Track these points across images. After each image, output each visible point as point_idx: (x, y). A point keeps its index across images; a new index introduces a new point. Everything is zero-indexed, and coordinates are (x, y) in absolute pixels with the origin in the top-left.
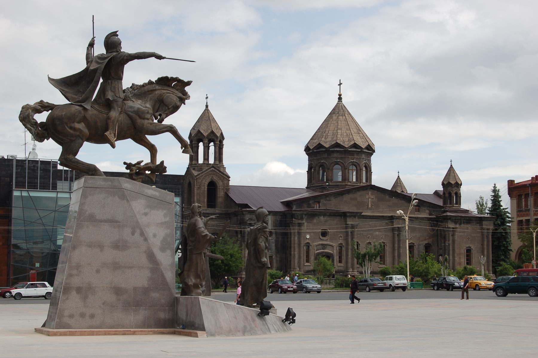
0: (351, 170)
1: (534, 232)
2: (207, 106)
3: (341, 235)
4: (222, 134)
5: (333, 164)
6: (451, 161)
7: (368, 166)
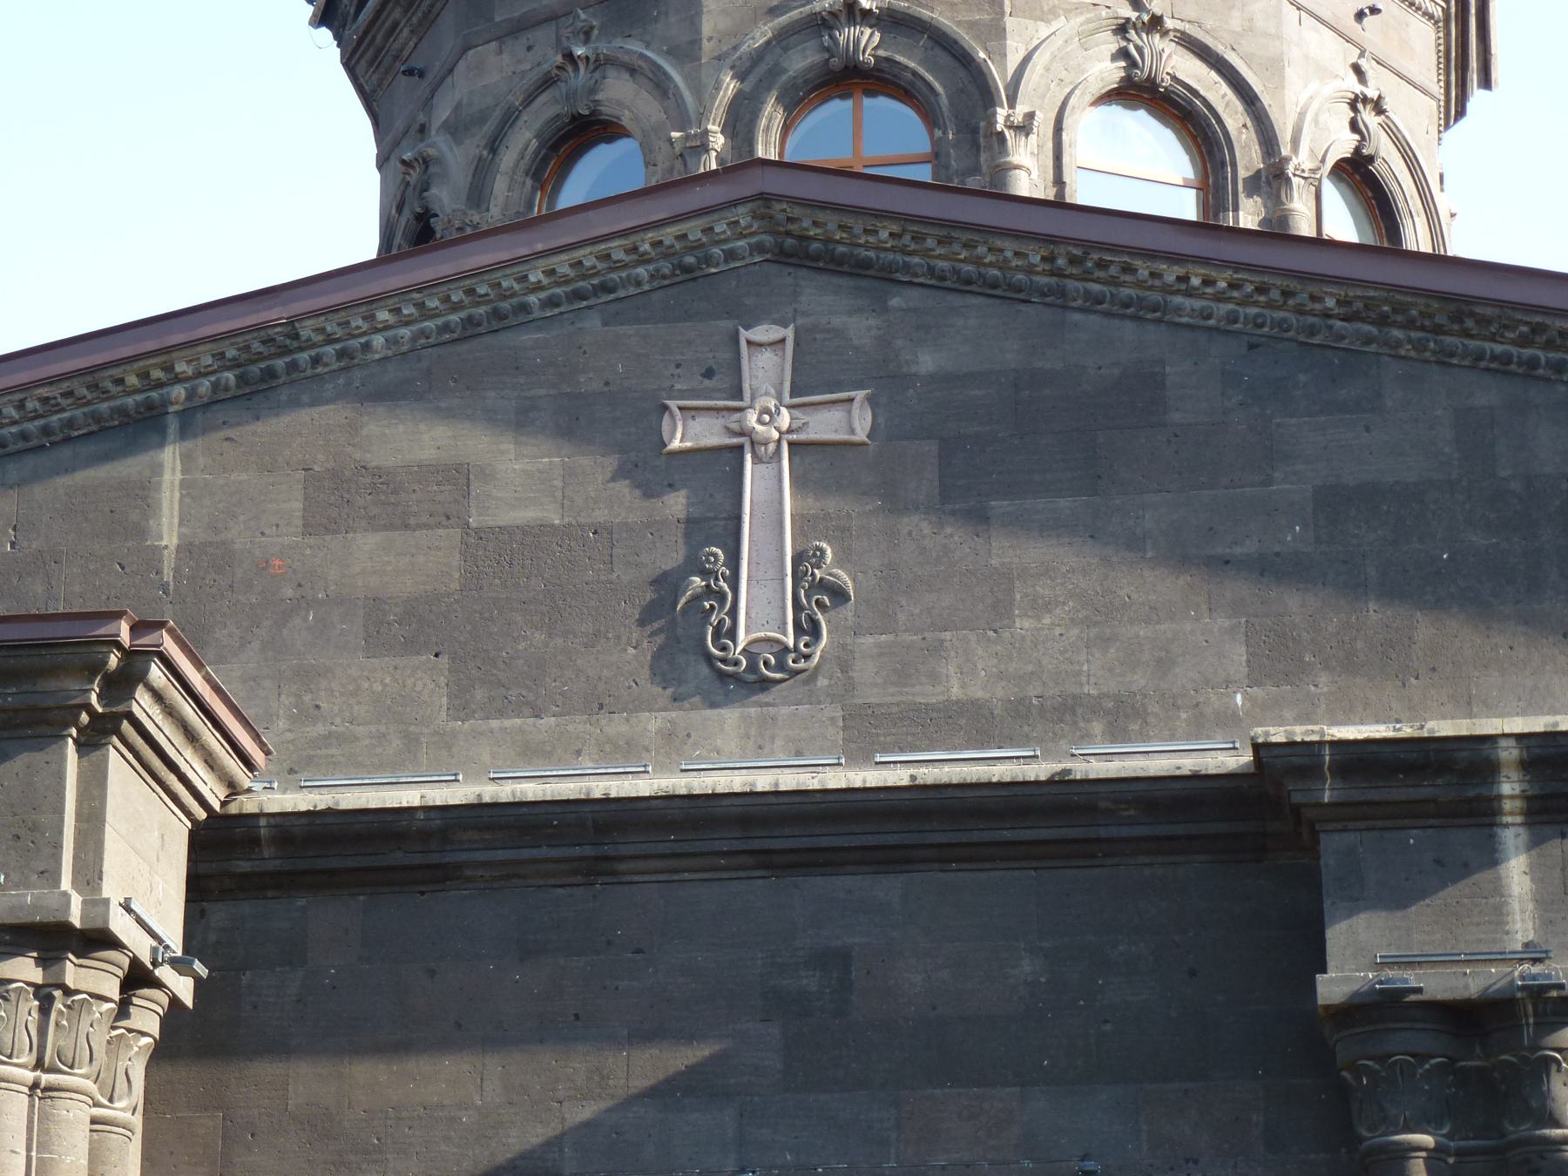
5: (523, 140)
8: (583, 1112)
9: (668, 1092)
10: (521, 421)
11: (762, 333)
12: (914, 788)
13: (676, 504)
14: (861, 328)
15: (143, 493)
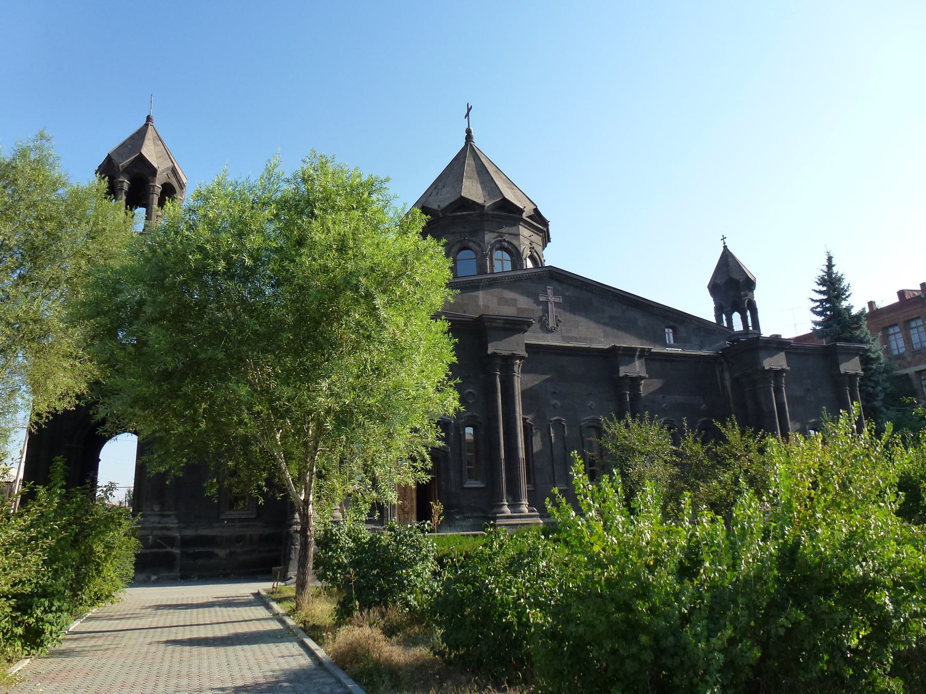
0: (499, 260)
3: (469, 390)
6: (724, 239)
8: (537, 383)
9: (546, 381)
10: (522, 294)
11: (549, 287)
12: (589, 348)
13: (541, 307)
14: (560, 288)
15: (477, 297)
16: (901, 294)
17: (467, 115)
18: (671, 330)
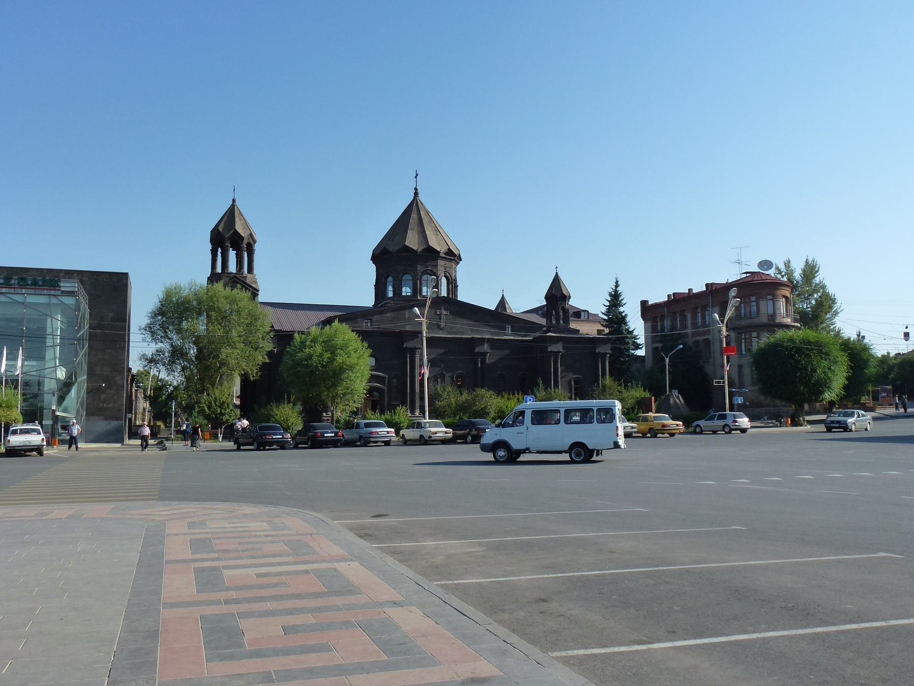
0: (425, 280)
1: (667, 357)
2: (234, 201)
4: (251, 235)
7: (449, 276)
16: (707, 285)
17: (416, 177)
18: (510, 326)
